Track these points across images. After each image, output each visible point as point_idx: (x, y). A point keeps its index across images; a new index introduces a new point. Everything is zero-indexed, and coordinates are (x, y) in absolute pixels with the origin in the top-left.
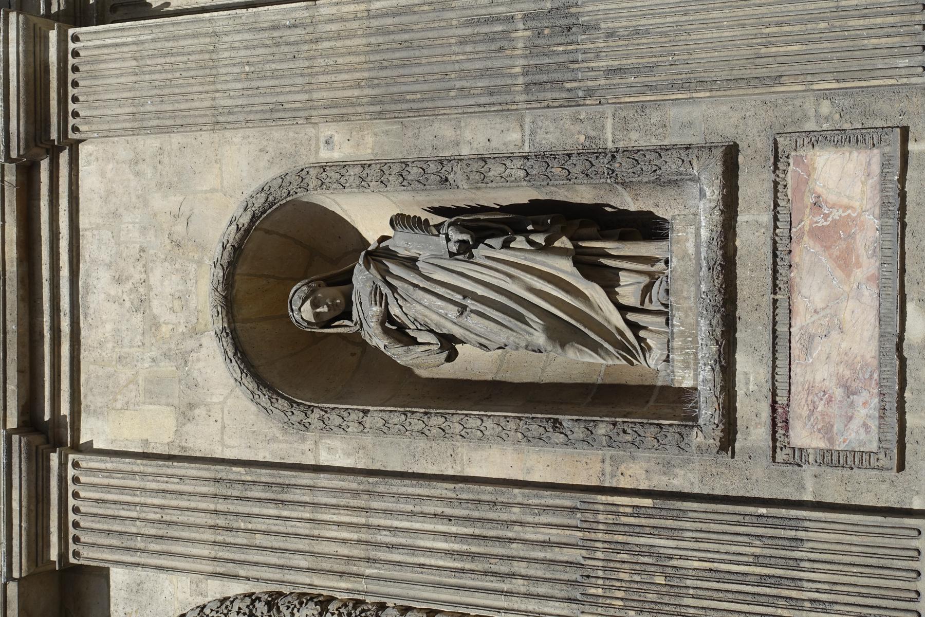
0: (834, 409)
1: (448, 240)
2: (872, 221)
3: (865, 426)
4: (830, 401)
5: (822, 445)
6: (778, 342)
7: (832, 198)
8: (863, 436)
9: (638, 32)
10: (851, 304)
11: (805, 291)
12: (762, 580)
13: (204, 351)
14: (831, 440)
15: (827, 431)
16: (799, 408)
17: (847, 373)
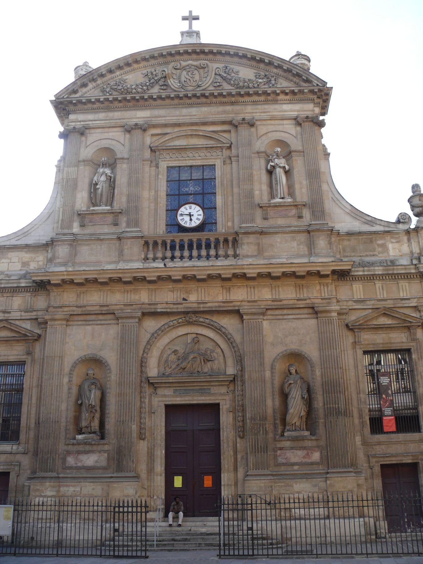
9: (337, 425)
12: (258, 448)
15: (280, 456)
16: (283, 451)
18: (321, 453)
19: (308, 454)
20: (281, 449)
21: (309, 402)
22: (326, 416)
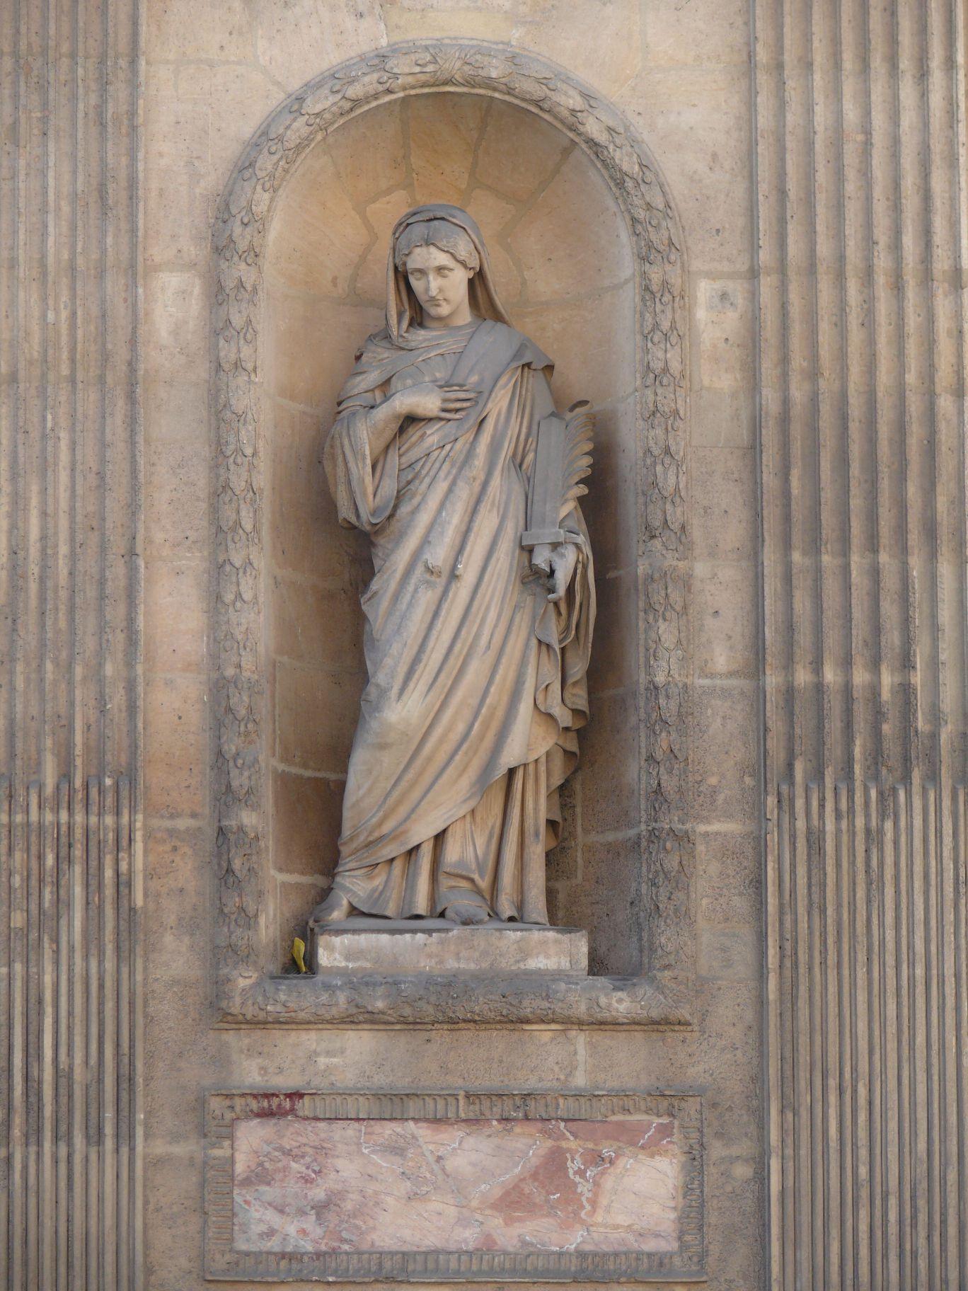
0: (293, 1187)
1: (555, 546)
2: (575, 1240)
3: (271, 1233)
4: (307, 1180)
5: (240, 1168)
6: (392, 1104)
7: (608, 1183)
8: (257, 1229)
9: (874, 882)
10: (452, 1211)
11: (471, 1142)
13: (349, 22)
14: (247, 1182)
15: (260, 1176)
16: (293, 1134)
17: (348, 1206)
18: (695, 1161)
19: (554, 1165)
20: (276, 1105)
21: (597, 623)
22: (766, 778)
